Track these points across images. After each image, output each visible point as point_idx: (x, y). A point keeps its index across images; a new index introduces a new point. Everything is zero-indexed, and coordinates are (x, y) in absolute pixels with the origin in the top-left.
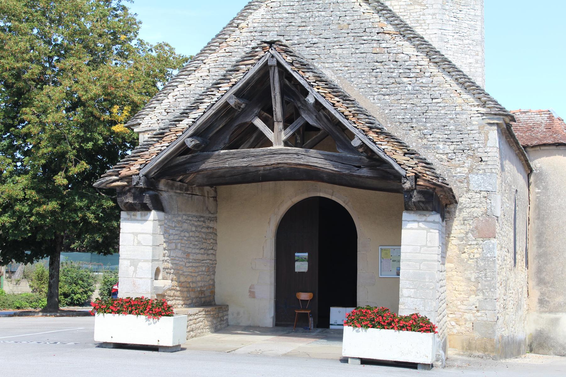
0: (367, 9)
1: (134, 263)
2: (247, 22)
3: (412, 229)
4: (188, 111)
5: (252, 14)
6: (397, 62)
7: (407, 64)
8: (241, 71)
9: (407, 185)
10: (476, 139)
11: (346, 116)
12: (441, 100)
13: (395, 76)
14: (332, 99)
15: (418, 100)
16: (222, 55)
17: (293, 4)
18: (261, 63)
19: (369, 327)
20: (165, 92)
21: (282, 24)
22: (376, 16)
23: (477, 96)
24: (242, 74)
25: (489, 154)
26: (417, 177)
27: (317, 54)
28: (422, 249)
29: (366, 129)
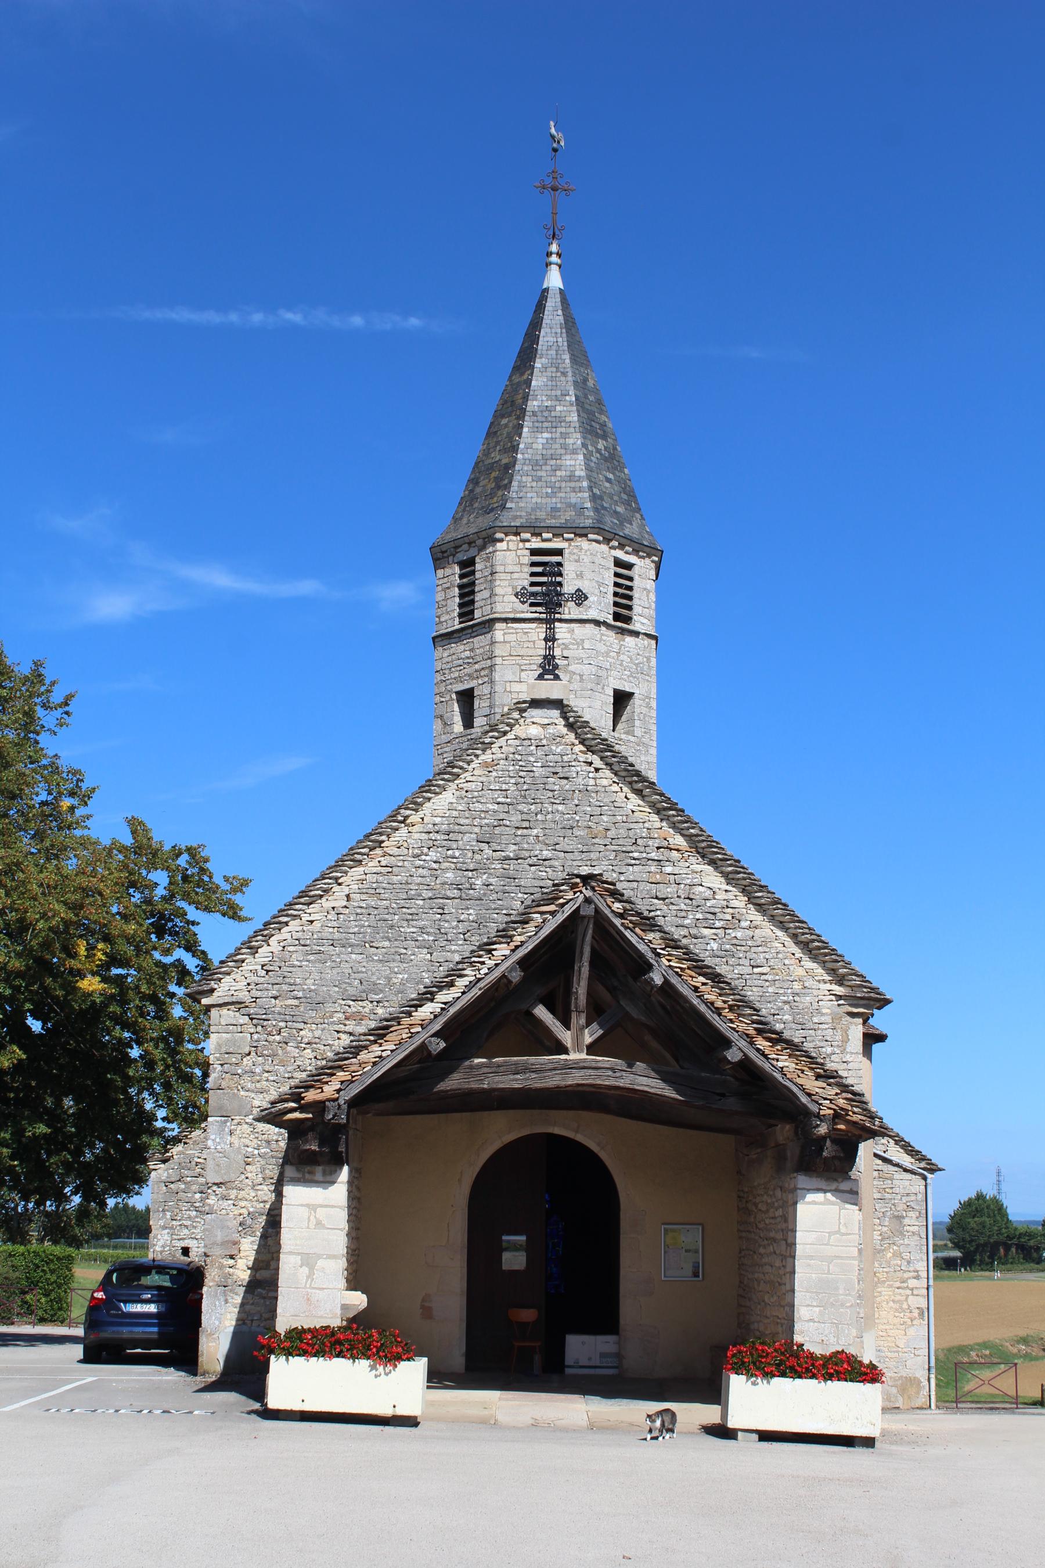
0: (639, 806)
1: (309, 1261)
2: (421, 814)
3: (814, 1203)
4: (434, 989)
5: (432, 801)
6: (691, 899)
7: (709, 904)
8: (532, 924)
9: (823, 1129)
10: (828, 1038)
11: (717, 1008)
12: (769, 969)
13: (689, 924)
14: (694, 979)
15: (728, 968)
16: (375, 870)
17: (507, 787)
18: (568, 910)
19: (774, 1376)
20: (266, 932)
21: (486, 821)
22: (655, 818)
23: (830, 965)
24: (534, 929)
25: (850, 1066)
26: (838, 1116)
27: (550, 880)
28: (832, 1237)
29: (752, 1032)
